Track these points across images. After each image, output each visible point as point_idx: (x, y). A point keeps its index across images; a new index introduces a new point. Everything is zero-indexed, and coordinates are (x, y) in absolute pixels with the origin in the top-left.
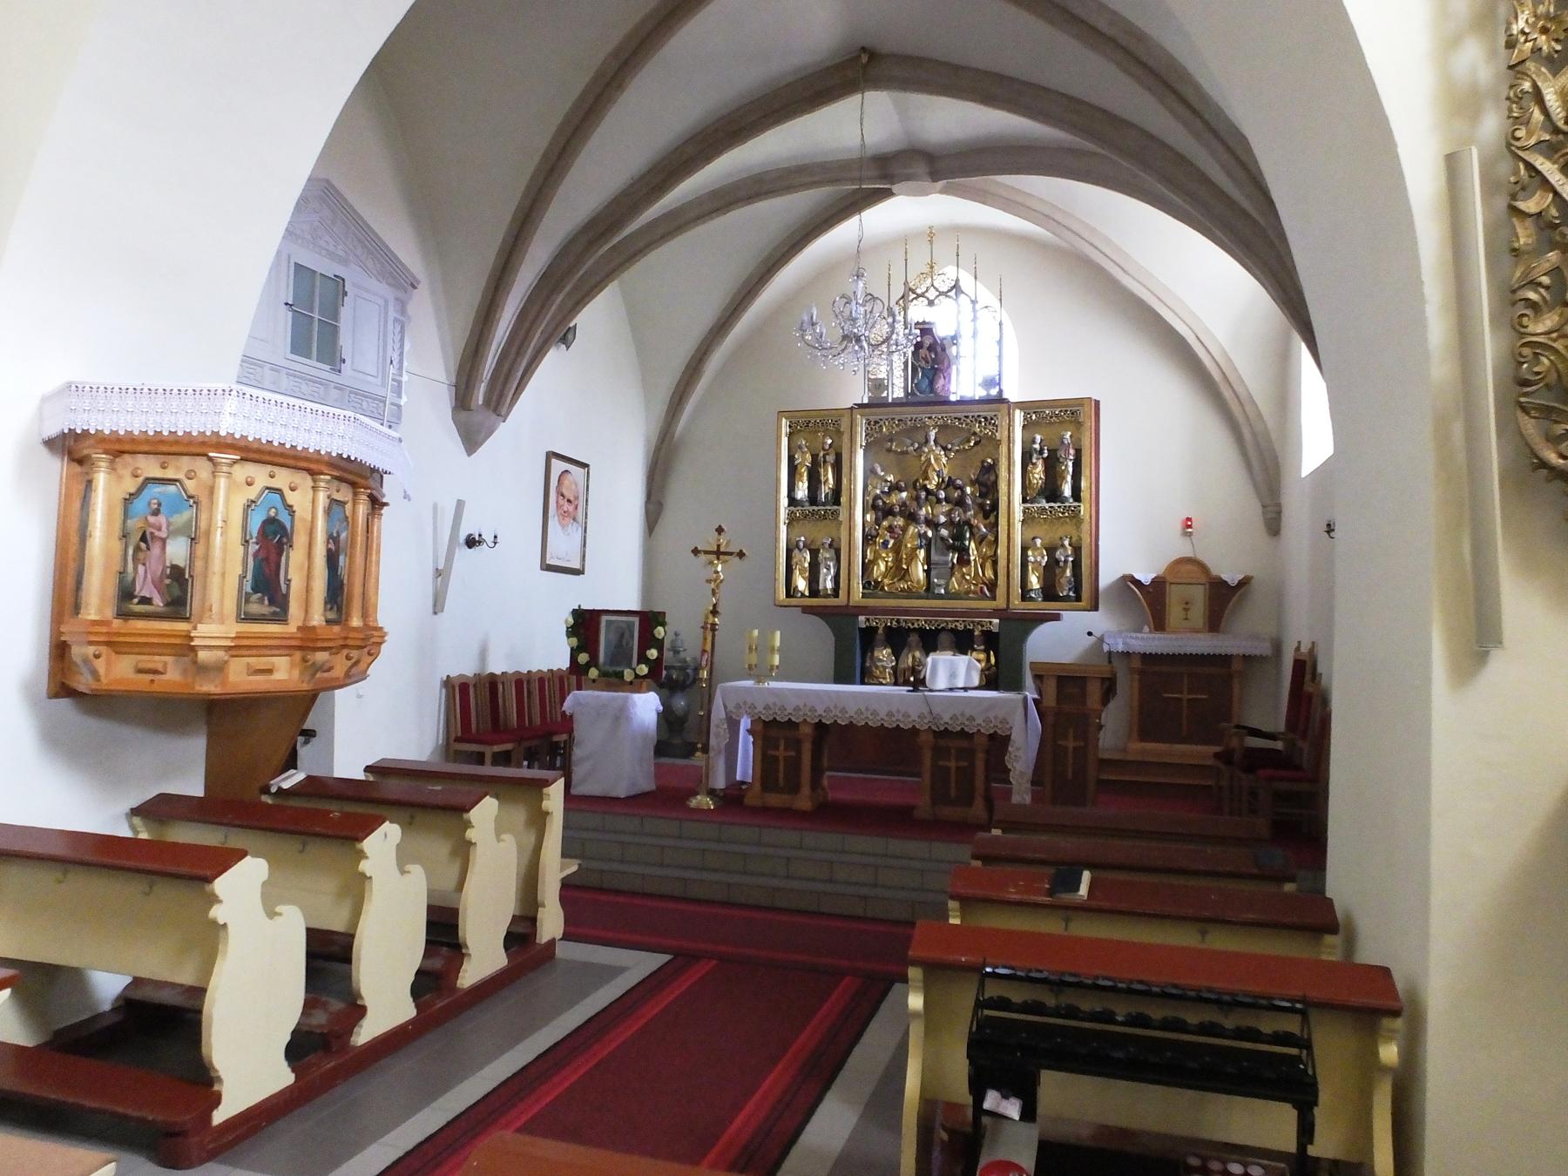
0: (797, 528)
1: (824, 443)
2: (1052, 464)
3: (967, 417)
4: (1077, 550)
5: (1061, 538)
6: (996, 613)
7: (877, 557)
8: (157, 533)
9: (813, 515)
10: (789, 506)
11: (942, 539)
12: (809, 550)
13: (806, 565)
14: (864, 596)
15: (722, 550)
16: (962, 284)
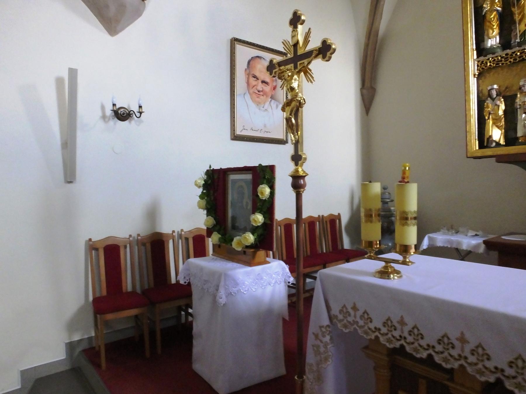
0: (489, 77)
9: (506, 59)
10: (478, 57)
13: (501, 113)
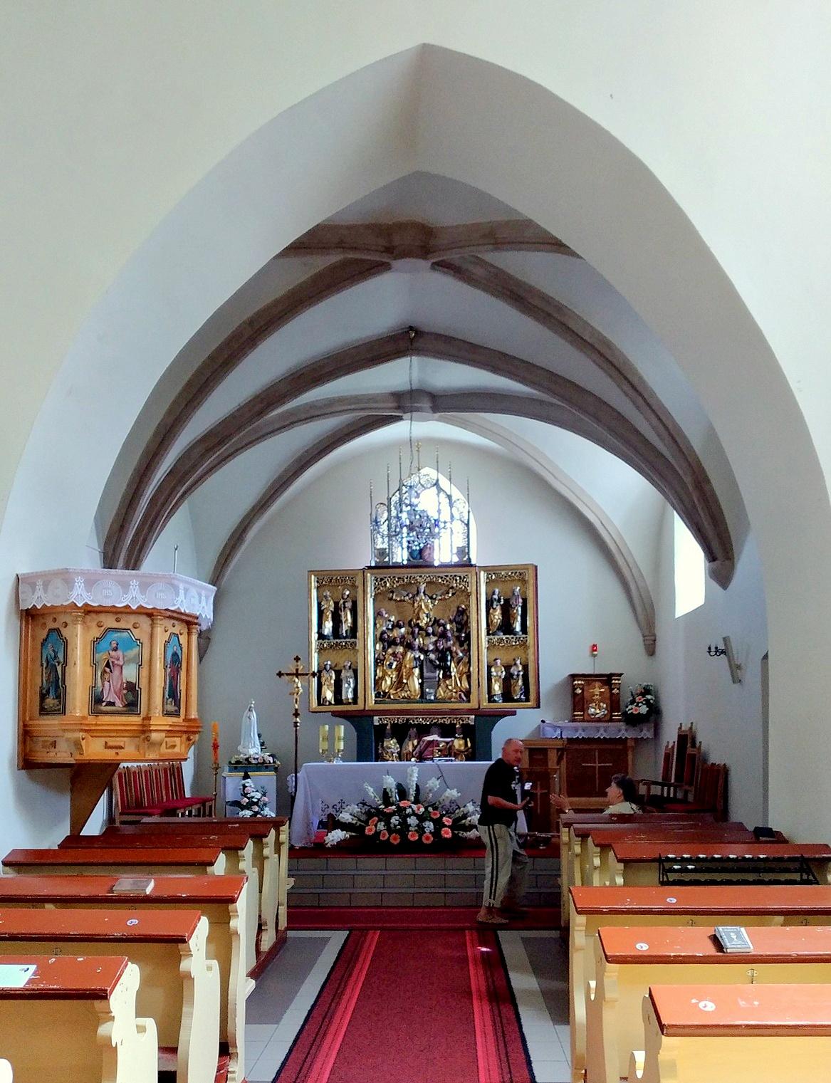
1: (343, 594)
2: (507, 609)
3: (447, 576)
4: (526, 667)
5: (514, 660)
6: (470, 711)
7: (385, 674)
8: (116, 662)
9: (336, 646)
11: (431, 661)
12: (334, 670)
13: (333, 682)
14: (376, 702)
15: (299, 672)
16: (440, 482)
